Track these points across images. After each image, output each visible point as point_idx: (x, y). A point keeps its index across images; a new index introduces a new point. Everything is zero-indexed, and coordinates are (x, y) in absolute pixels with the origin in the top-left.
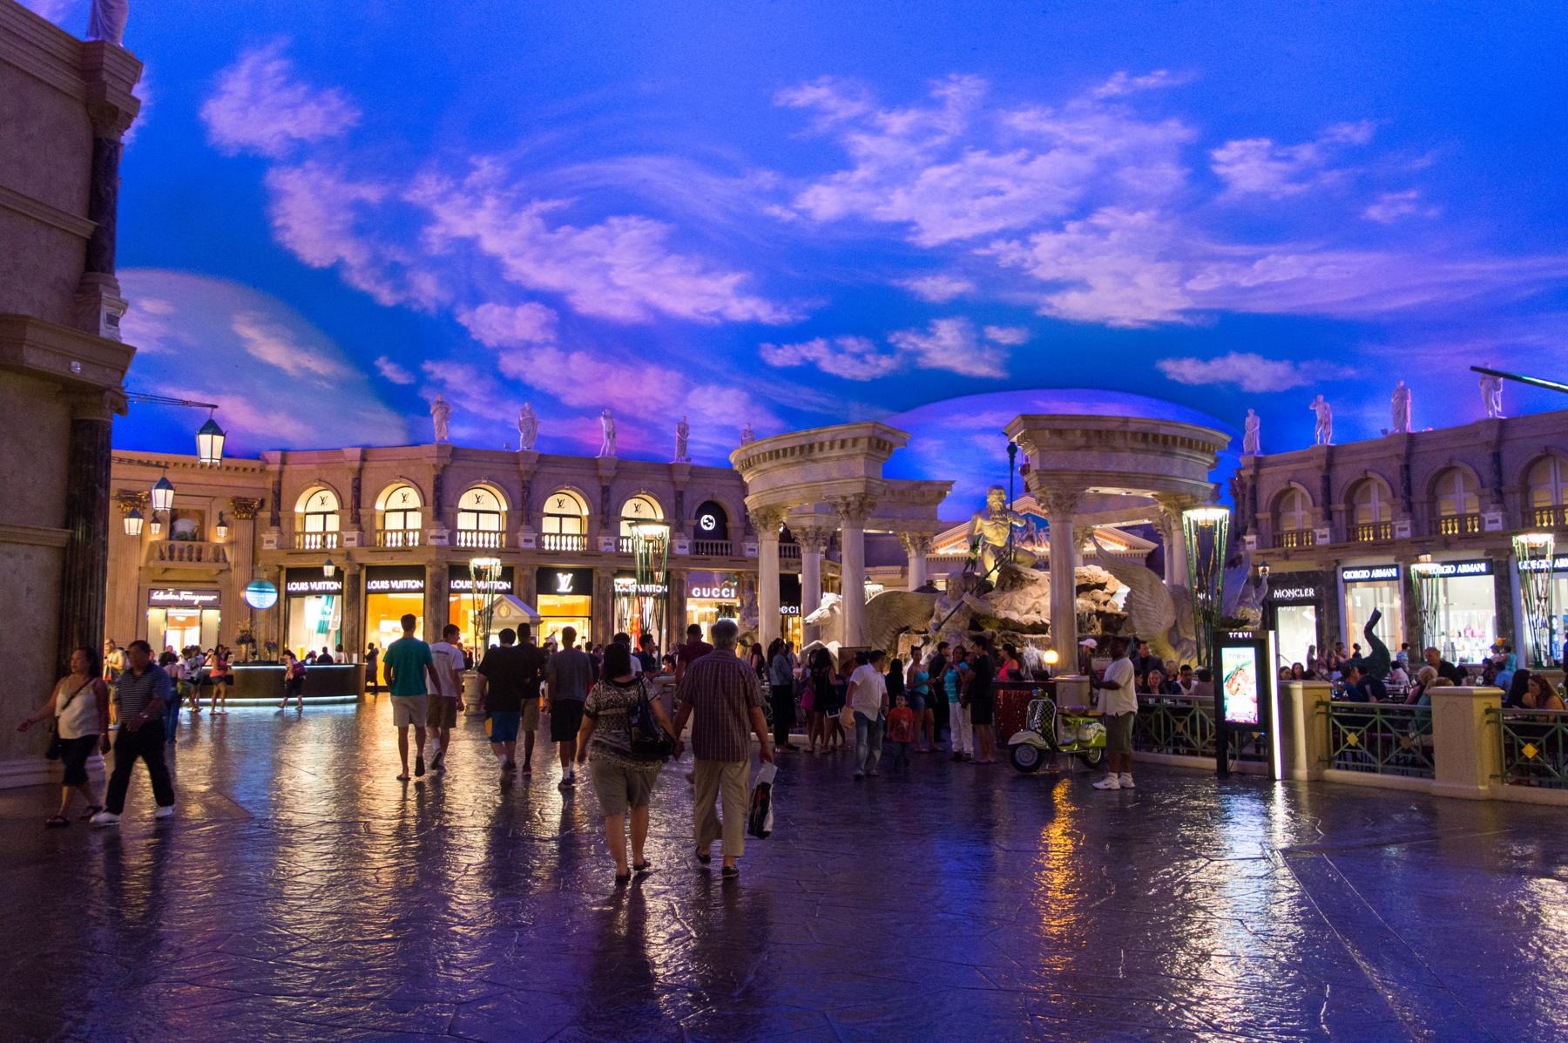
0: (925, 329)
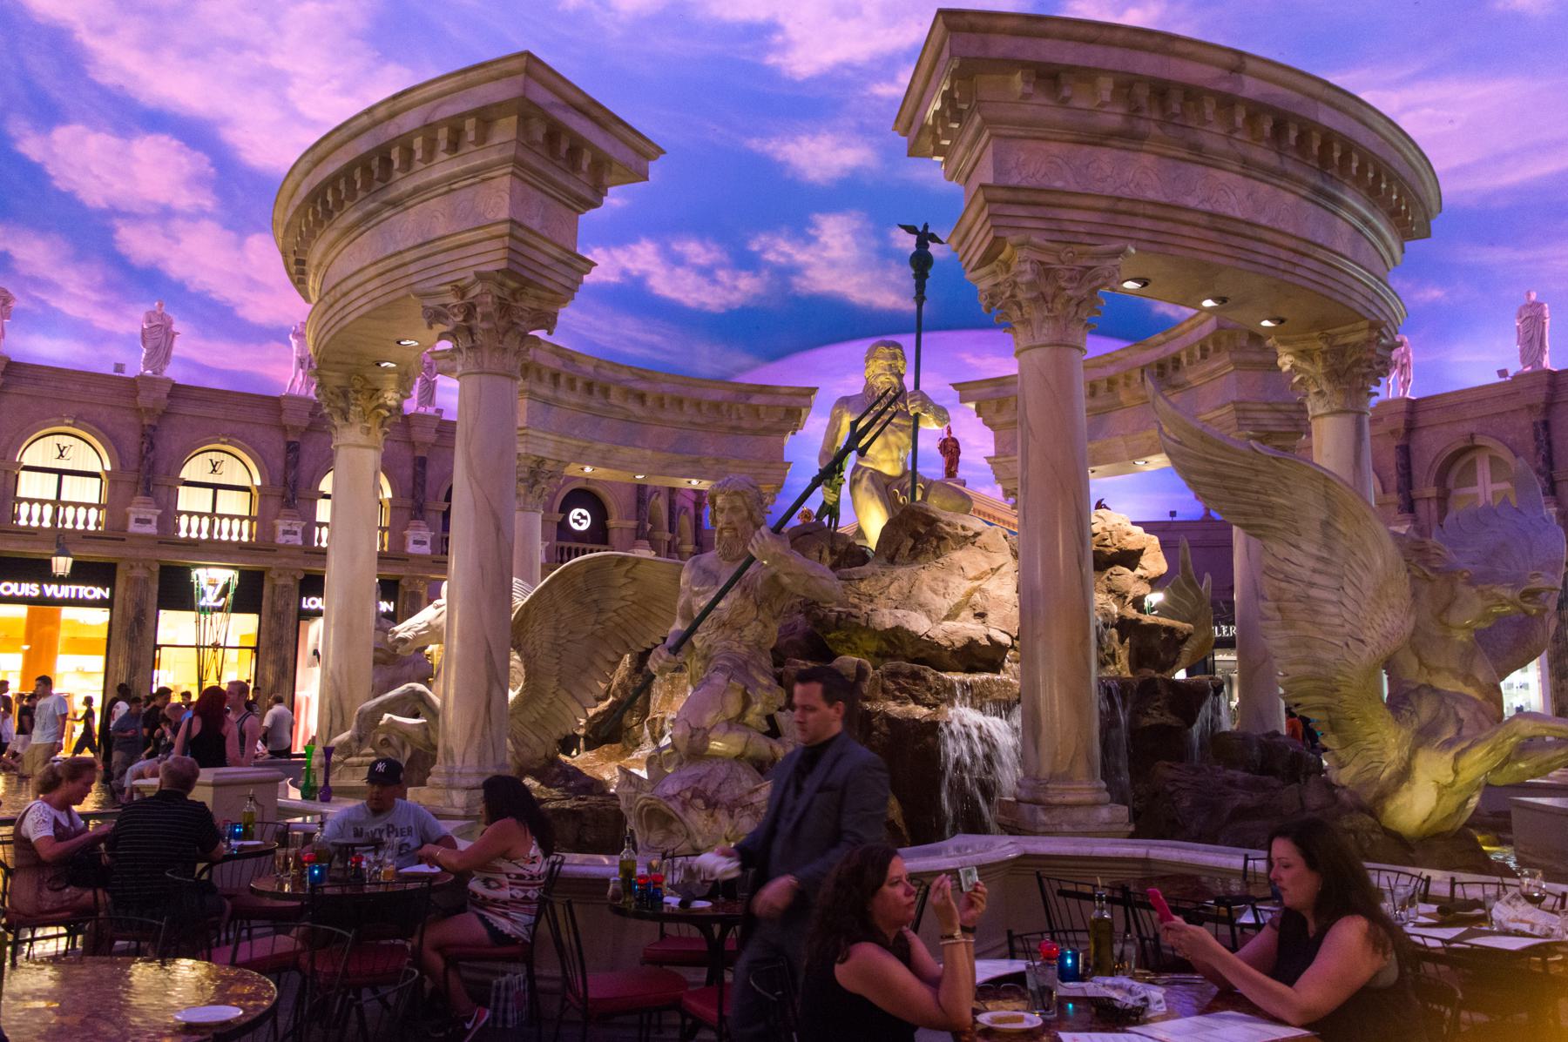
0: (803, 232)
